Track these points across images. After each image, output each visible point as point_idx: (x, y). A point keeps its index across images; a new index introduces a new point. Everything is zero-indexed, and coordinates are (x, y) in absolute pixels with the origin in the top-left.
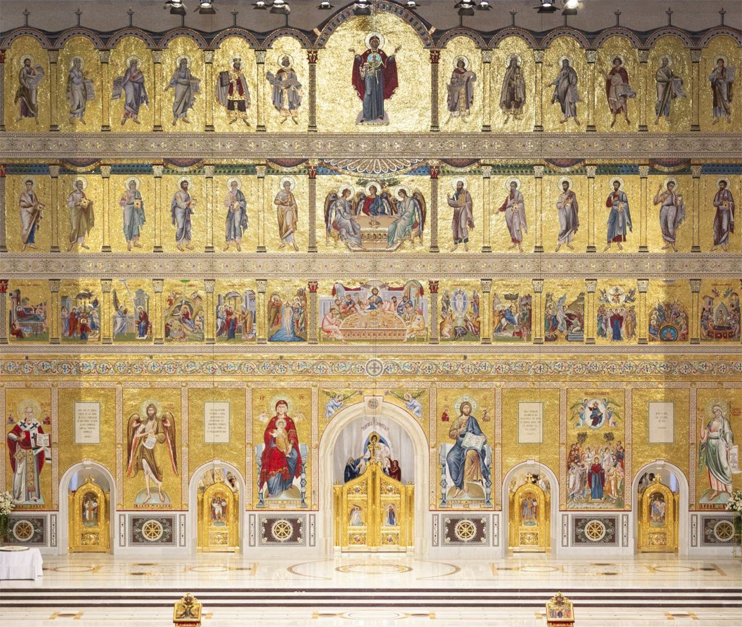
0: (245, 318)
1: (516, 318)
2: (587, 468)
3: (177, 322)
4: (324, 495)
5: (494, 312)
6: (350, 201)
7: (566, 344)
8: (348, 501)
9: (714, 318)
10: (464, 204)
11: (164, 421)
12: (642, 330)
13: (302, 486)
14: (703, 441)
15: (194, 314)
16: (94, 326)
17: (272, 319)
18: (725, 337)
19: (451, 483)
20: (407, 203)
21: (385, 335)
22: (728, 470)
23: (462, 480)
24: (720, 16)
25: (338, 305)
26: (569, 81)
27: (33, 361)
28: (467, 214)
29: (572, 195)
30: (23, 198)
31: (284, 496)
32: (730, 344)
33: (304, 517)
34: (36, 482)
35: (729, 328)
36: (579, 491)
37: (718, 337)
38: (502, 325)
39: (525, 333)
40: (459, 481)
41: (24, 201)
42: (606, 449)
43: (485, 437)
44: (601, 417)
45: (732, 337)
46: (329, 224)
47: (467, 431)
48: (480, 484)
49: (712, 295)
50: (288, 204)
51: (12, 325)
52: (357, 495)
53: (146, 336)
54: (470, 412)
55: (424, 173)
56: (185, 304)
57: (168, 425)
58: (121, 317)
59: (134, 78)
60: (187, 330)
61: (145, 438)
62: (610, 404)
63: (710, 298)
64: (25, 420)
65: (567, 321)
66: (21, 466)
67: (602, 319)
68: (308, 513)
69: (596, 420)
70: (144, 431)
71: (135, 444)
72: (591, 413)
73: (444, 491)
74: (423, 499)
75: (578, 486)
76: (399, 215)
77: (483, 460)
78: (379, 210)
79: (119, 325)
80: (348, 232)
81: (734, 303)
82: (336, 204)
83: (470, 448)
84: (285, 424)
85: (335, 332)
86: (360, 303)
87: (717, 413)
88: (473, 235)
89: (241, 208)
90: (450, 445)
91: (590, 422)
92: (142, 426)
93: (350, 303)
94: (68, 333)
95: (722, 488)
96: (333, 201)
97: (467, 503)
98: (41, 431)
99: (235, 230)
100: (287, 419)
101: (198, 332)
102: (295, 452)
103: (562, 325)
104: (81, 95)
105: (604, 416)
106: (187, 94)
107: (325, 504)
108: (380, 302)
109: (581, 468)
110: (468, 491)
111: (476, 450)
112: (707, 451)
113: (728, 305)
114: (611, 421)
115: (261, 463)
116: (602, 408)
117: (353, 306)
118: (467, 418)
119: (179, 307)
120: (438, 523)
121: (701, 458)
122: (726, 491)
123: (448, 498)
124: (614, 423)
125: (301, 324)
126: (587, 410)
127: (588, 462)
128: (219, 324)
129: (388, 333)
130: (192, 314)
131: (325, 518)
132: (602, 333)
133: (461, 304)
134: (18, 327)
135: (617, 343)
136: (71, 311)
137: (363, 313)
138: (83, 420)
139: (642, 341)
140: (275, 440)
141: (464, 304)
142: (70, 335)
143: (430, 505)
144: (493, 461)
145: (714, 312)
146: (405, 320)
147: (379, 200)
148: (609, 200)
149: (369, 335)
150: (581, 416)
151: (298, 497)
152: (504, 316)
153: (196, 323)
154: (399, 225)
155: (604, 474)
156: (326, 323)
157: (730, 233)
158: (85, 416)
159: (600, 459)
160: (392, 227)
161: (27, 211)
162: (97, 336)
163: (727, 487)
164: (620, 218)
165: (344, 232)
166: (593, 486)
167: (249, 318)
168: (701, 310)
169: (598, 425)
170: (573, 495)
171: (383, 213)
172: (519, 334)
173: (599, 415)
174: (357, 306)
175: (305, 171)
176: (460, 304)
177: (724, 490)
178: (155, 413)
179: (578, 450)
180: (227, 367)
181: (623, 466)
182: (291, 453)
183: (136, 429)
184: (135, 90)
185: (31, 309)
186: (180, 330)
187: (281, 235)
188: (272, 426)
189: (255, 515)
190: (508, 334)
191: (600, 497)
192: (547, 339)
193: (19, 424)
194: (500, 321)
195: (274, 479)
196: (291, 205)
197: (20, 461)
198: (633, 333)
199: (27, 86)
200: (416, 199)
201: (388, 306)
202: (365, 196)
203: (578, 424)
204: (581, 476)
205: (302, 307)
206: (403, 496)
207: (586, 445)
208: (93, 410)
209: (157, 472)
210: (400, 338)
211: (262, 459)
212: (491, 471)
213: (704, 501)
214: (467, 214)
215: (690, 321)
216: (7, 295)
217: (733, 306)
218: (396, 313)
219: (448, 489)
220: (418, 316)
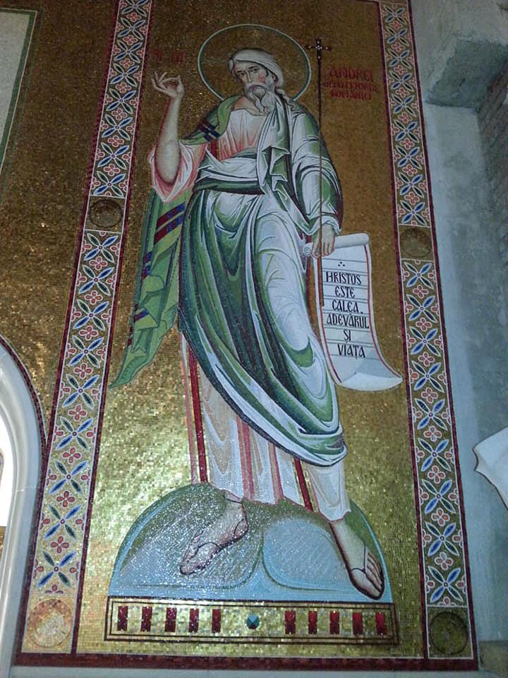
14: (168, 199)
22: (318, 367)
112: (187, 255)
121: (151, 284)
122: (309, 508)
163: (310, 474)
177: (297, 498)
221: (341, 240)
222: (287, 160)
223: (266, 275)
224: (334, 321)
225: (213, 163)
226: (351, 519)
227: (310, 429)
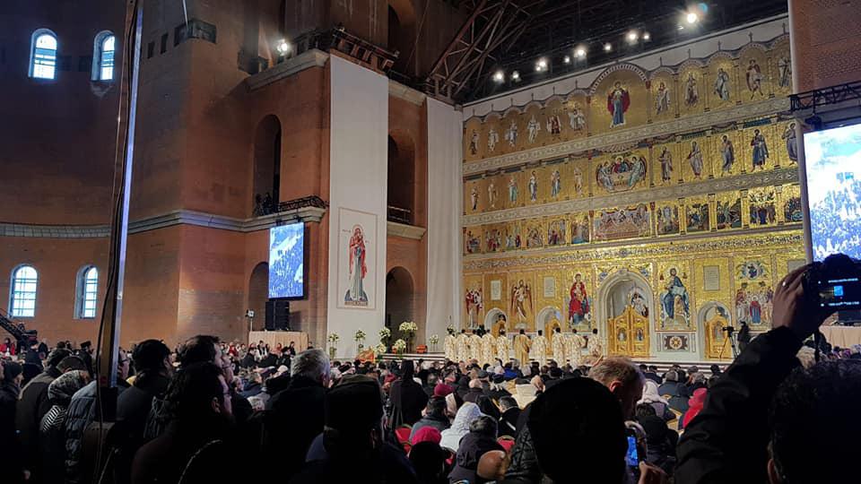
2: (749, 304)
7: (731, 229)
29: (729, 143)
39: (705, 226)
55: (644, 146)
69: (753, 274)
88: (671, 174)
108: (625, 217)
116: (756, 266)
123: (665, 324)
132: (753, 221)
135: (763, 226)
137: (616, 224)
148: (753, 141)
176: (667, 213)
188: (574, 288)
190: (696, 227)
191: (759, 322)
204: (745, 310)
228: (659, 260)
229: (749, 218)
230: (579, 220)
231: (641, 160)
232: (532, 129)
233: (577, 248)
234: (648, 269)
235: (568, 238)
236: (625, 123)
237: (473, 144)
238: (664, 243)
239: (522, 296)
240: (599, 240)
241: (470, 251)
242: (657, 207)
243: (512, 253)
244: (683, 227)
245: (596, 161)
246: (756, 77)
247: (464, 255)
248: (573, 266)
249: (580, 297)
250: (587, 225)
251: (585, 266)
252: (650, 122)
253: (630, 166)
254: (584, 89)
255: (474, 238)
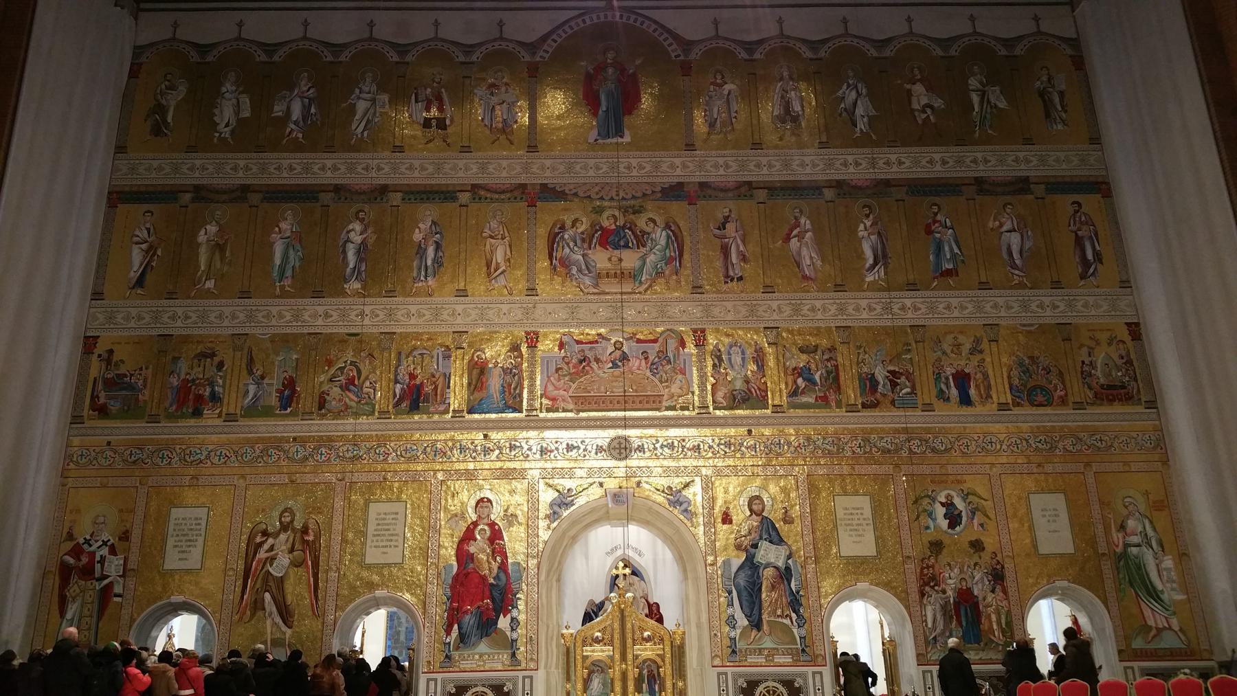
0: (434, 383)
1: (817, 377)
3: (337, 390)
4: (547, 643)
5: (786, 369)
6: (582, 233)
8: (585, 658)
9: (1099, 374)
10: (733, 235)
11: (305, 530)
12: (1002, 393)
13: (513, 630)
14: (1119, 550)
15: (362, 378)
16: (215, 398)
17: (474, 383)
18: (1120, 400)
19: (742, 621)
20: (658, 234)
21: (633, 402)
23: (760, 614)
24: (1033, 22)
25: (567, 364)
26: (858, 92)
27: (117, 448)
28: (738, 247)
30: (137, 233)
31: (483, 647)
32: (1129, 409)
33: (514, 681)
34: (93, 632)
35: (1123, 387)
36: (943, 633)
37: (1111, 401)
38: (798, 387)
39: (832, 397)
40: (755, 617)
41: (138, 236)
42: (976, 564)
43: (789, 547)
44: (960, 515)
45: (1131, 398)
46: (554, 261)
47: (761, 538)
48: (787, 621)
49: (1092, 344)
50: (500, 236)
51: (94, 397)
52: (597, 647)
53: (289, 410)
54: (763, 510)
56: (351, 365)
57: (311, 538)
58: (257, 383)
59: (303, 92)
60: (351, 400)
61: (273, 559)
62: (970, 497)
63: (1089, 347)
64: (91, 536)
65: (891, 381)
66: (75, 607)
67: (940, 377)
68: (521, 674)
69: (954, 519)
70: (272, 548)
71: (256, 569)
72: (944, 510)
73: (732, 634)
74: (700, 649)
75: (940, 626)
76: (648, 249)
77: (789, 585)
78: (622, 243)
79: (251, 395)
80: (580, 270)
81: (1124, 353)
82: (563, 237)
83: (767, 565)
84: (488, 533)
85: (564, 400)
86: (597, 360)
87: (1131, 508)
89: (436, 242)
90: (738, 560)
91: (944, 524)
92: (270, 541)
93: (584, 360)
94: (174, 407)
95: (1162, 623)
96: (559, 233)
97: (772, 653)
98: (113, 551)
99: (426, 270)
100: (492, 525)
101: (366, 404)
102: (502, 576)
103: (884, 386)
104: (232, 111)
105: (964, 514)
106: (372, 111)
107: (547, 658)
108: (624, 358)
109: (941, 595)
110: (770, 634)
111: (777, 568)
113: (1115, 357)
114: (976, 521)
115: (449, 594)
116: (959, 503)
117: (588, 365)
118: (759, 518)
119: (341, 369)
120: (727, 687)
121: (1121, 576)
122: (1170, 628)
123: (740, 645)
124: (982, 525)
125: (515, 389)
126: (938, 506)
127: (951, 583)
128: (398, 391)
129: (637, 400)
130: (359, 378)
131: (548, 681)
132: (943, 396)
133: (739, 360)
134: (102, 400)
135: (966, 411)
136: (183, 377)
137: (603, 372)
138: (180, 533)
139: (1003, 407)
140: (471, 557)
141: (743, 359)
142: (176, 410)
143: (712, 658)
144: (803, 584)
145: (1099, 366)
146: (661, 382)
147: (621, 231)
149: (611, 403)
150: (930, 515)
151: (506, 648)
152: (800, 375)
153: (365, 390)
154: (648, 260)
155: (977, 604)
156: (550, 388)
157: (1099, 266)
158: (183, 527)
159: (969, 580)
160: (638, 264)
161: (141, 248)
162: (217, 411)
164: (947, 248)
165: (574, 270)
166: (964, 624)
167: (440, 382)
168: (1079, 365)
169: (958, 528)
170: (935, 638)
171: (626, 246)
172: (825, 399)
173: (956, 513)
174: (594, 365)
175: (522, 198)
176: (737, 359)
178: (292, 521)
179: (933, 567)
180: (406, 450)
181: (1005, 592)
182: (497, 578)
183: (261, 545)
184: (304, 106)
185: (125, 376)
186: (340, 400)
187: (489, 275)
188: (469, 536)
189: (436, 680)
190: (809, 399)
192: (864, 406)
193: (81, 541)
194: (795, 382)
195: (469, 620)
196: (503, 239)
197: (74, 599)
198: (989, 396)
199: (164, 102)
200: (670, 228)
201: (637, 364)
202: (601, 227)
203: (927, 528)
204: (944, 608)
205: (516, 367)
206: (668, 649)
207: (944, 558)
208: (196, 519)
209: (286, 613)
210: (654, 406)
211: (453, 587)
212: (803, 601)
213: (1138, 643)
214: (738, 247)
215: (1067, 378)
216: (95, 356)
217: (1122, 358)
218: (648, 374)
219: (739, 631)
220: (680, 377)
221: (1165, 558)
222: (1146, 535)
223: (1148, 570)
224: (1167, 581)
225: (1127, 539)
226: (1181, 630)
227: (1168, 610)
228: (719, 473)
229: (934, 392)
230: (495, 352)
231: (667, 226)
232: (361, 106)
233: (486, 427)
234: (688, 493)
235: (457, 397)
236: (627, 139)
237: (161, 109)
238: (732, 431)
239: (284, 560)
240: (548, 410)
241: (102, 411)
242: (712, 340)
243: (265, 427)
244: (777, 393)
245: (549, 214)
246: (924, 101)
247: (76, 419)
248: (470, 476)
249: (487, 565)
250: (518, 366)
251: (507, 475)
252: (690, 147)
253: (641, 240)
254: (522, 44)
255: (122, 370)
